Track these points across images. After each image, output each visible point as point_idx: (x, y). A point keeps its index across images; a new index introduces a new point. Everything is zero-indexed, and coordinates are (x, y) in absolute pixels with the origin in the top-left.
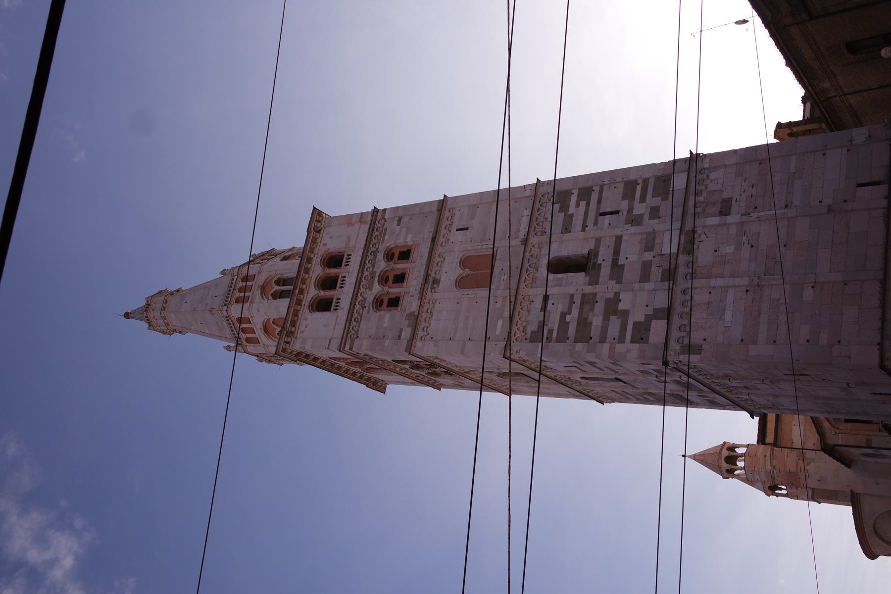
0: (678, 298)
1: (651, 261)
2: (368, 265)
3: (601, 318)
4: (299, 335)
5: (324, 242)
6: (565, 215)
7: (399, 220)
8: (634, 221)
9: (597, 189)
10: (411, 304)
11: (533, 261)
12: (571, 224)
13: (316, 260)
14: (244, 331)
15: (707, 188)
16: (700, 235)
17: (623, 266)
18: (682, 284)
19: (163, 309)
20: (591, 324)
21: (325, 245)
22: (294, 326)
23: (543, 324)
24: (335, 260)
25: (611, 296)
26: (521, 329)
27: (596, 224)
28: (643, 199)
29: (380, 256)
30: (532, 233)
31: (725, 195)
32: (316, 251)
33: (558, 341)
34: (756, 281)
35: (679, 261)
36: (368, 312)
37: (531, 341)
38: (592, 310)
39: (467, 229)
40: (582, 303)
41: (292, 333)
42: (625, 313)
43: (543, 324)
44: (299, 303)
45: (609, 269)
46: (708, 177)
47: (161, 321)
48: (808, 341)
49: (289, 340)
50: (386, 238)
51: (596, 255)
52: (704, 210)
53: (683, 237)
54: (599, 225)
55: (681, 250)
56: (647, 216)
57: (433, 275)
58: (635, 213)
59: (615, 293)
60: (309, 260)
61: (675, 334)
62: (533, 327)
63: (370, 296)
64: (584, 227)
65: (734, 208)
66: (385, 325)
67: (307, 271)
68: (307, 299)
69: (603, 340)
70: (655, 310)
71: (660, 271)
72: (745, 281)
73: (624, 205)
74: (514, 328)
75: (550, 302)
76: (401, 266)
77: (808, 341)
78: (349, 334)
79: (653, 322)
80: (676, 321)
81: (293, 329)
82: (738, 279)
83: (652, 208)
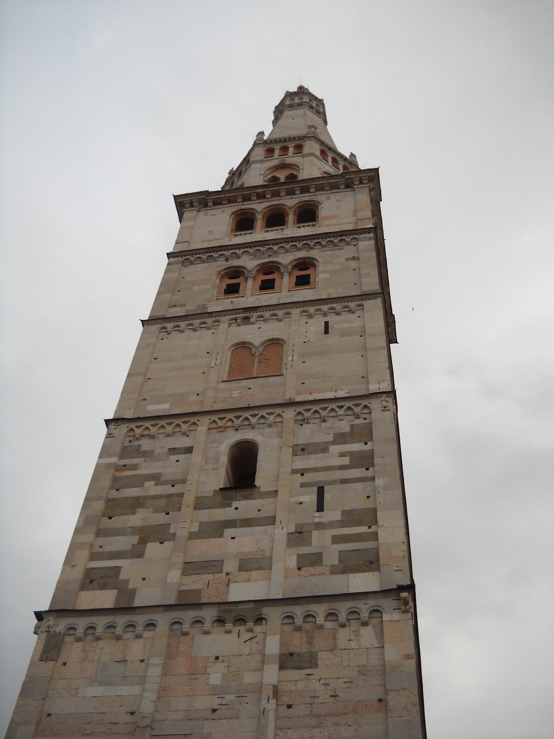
0: (140, 619)
1: (221, 572)
3: (139, 524)
4: (202, 213)
7: (354, 258)
8: (299, 536)
9: (369, 474)
11: (253, 420)
12: (310, 453)
13: (306, 197)
15: (343, 626)
16: (251, 631)
17: (221, 536)
18: (163, 620)
20: (134, 513)
23: (146, 454)
24: (308, 214)
25: (172, 531)
26: (146, 432)
27: (303, 485)
28: (336, 540)
29: (302, 254)
30: (301, 409)
31: (324, 658)
33: (115, 479)
34: (146, 722)
36: (218, 267)
37: (124, 449)
39: (327, 331)
41: (206, 206)
43: (146, 454)
44: (247, 198)
45: (222, 518)
46: (365, 624)
50: (328, 253)
51: (246, 498)
52: (299, 629)
53: (251, 606)
54: (302, 490)
55: (227, 607)
56: (306, 550)
58: (315, 534)
59: (174, 534)
60: (305, 190)
61: (81, 623)
62: (146, 444)
67: (290, 193)
69: (99, 533)
70: (134, 591)
71: (200, 587)
72: (147, 706)
73: (332, 514)
74: (148, 424)
75: (182, 457)
79: (114, 592)
80: (101, 622)
81: (210, 204)
82: (153, 696)
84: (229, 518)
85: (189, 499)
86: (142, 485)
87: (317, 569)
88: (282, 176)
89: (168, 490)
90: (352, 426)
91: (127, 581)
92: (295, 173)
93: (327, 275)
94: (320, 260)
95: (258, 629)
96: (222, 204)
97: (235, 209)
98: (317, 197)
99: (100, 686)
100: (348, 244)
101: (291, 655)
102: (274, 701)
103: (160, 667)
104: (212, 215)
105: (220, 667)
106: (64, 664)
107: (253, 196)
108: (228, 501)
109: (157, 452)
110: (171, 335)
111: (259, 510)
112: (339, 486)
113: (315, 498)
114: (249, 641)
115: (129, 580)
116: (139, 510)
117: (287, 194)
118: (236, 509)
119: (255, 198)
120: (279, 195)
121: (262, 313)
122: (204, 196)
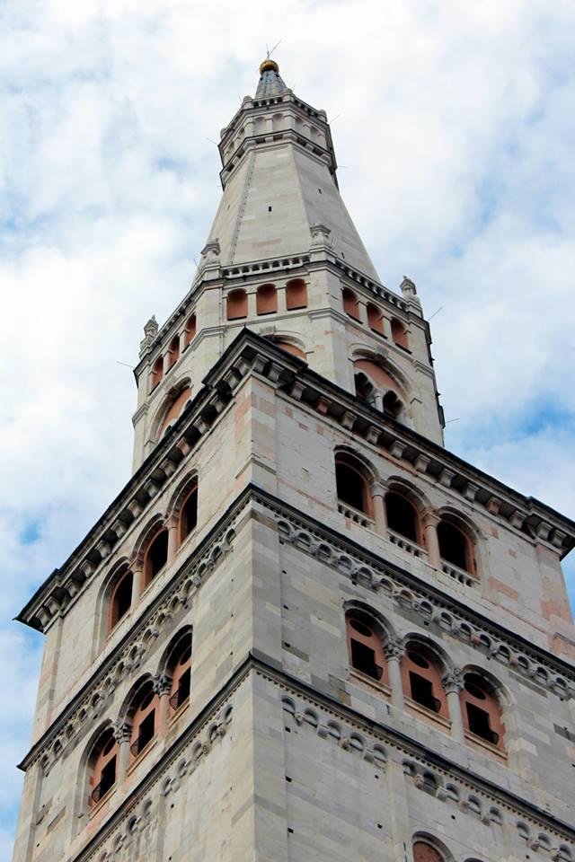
2: (458, 623)
5: (500, 530)
10: (363, 698)
13: (459, 503)
14: (266, 292)
19: (302, 142)
21: (495, 535)
22: (304, 399)
24: (457, 544)
29: (479, 659)
32: (476, 506)
36: (342, 587)
44: (361, 429)
47: (267, 127)
49: (273, 374)
50: (524, 688)
57: (446, 779)
60: (459, 485)
63: (382, 602)
66: (314, 619)
67: (435, 472)
68: (366, 449)
76: (454, 704)
78: (292, 523)
81: (297, 393)
88: (380, 387)
92: (400, 397)
93: (532, 749)
94: (514, 699)
96: (314, 405)
97: (340, 443)
98: (475, 514)
100: (551, 688)
104: (301, 425)
107: (374, 434)
110: (300, 730)
117: (429, 472)
119: (375, 439)
120: (413, 461)
121: (456, 784)
122: (296, 372)
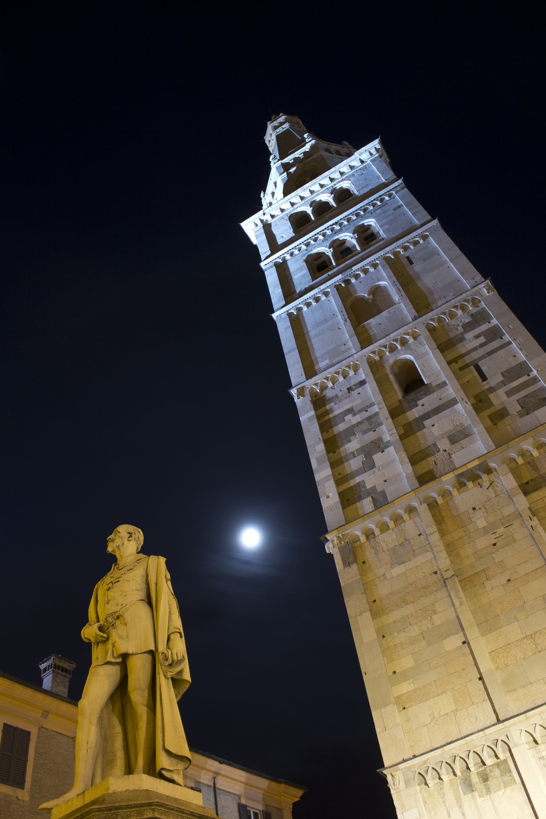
1: (439, 451)
3: (359, 446)
6: (462, 333)
8: (480, 403)
17: (424, 427)
20: (350, 441)
27: (461, 369)
34: (450, 573)
35: (445, 478)
38: (364, 432)
40: (369, 418)
42: (373, 466)
48: (395, 672)
50: (377, 212)
62: (329, 393)
64: (455, 360)
65: (535, 496)
75: (360, 390)
77: (395, 672)
79: (369, 499)
82: (444, 554)
83: (504, 409)
84: (422, 413)
85: (384, 414)
86: (344, 421)
87: (507, 420)
89: (365, 415)
90: (472, 315)
91: (374, 488)
95: (492, 477)
99: (399, 565)
101: (527, 483)
102: (535, 519)
103: (437, 533)
105: (479, 513)
106: (364, 562)
108: (414, 403)
109: (340, 394)
111: (440, 399)
112: (488, 358)
113: (475, 373)
114: (491, 488)
115: (375, 486)
116: (352, 438)
118: (423, 405)
